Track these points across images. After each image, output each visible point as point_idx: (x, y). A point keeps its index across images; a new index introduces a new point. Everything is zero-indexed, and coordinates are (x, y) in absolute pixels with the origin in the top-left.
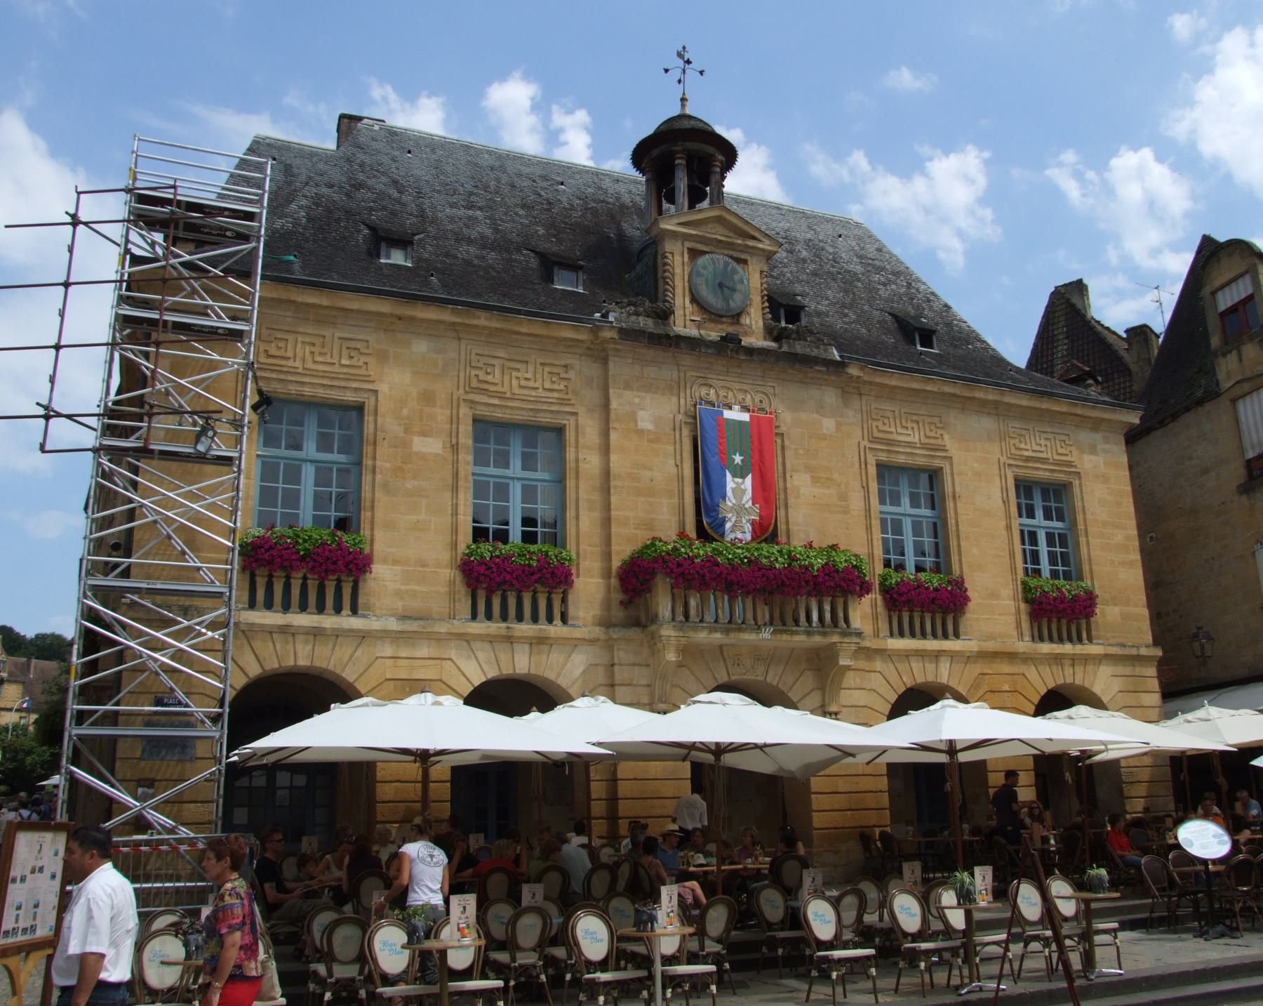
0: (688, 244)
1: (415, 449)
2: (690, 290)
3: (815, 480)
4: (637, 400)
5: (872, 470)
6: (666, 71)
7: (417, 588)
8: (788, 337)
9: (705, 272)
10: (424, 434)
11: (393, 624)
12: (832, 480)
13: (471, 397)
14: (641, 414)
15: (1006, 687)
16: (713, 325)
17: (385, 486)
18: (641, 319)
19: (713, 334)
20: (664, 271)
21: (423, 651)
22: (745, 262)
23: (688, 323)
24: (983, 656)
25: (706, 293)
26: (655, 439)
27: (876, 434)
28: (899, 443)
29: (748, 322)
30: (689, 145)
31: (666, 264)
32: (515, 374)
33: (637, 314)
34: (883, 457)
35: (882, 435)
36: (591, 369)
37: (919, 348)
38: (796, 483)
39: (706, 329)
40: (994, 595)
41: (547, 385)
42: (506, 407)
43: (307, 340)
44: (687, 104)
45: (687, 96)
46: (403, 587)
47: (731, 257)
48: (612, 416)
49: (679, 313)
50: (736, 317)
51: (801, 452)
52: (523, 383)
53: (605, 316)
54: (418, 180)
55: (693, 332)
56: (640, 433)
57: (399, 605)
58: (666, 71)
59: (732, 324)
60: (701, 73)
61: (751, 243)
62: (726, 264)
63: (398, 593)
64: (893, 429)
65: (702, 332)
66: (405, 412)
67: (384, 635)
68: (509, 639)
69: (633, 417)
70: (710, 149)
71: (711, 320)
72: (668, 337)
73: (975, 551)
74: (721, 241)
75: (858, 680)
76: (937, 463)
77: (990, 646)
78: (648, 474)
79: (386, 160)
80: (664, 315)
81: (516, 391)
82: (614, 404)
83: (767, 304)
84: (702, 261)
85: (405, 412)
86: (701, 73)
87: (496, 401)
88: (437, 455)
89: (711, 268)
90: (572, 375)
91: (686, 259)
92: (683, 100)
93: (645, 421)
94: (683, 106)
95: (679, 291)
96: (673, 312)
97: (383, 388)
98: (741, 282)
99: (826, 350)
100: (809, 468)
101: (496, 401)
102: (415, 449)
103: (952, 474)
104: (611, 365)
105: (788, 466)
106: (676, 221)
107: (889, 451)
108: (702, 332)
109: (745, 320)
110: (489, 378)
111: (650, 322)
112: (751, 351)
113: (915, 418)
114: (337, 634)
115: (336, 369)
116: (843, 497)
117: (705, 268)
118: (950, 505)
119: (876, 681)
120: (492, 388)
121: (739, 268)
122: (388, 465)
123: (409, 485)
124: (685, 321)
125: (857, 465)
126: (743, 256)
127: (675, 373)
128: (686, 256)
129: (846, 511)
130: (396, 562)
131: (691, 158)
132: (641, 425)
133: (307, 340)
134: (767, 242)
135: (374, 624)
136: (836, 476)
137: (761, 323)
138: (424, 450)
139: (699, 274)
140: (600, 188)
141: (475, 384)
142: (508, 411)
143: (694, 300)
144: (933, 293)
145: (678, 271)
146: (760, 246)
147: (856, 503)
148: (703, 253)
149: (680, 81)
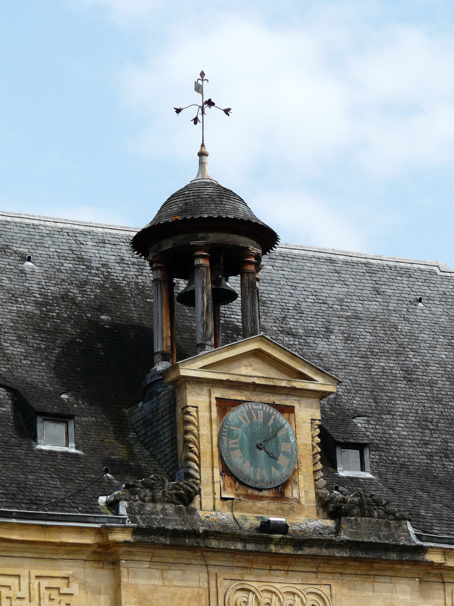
0: (218, 393)
2: (221, 457)
6: (178, 111)
8: (347, 514)
9: (239, 431)
16: (250, 503)
18: (159, 507)
19: (249, 517)
20: (187, 432)
22: (290, 410)
23: (218, 502)
25: (240, 461)
29: (295, 495)
30: (213, 238)
31: (188, 422)
33: (154, 500)
36: (100, 577)
44: (207, 160)
45: (207, 149)
47: (273, 405)
49: (206, 489)
50: (280, 492)
53: (113, 506)
55: (224, 515)
58: (178, 111)
59: (274, 499)
60: (227, 111)
61: (299, 384)
62: (267, 417)
65: (237, 514)
70: (243, 241)
72: (194, 534)
74: (259, 385)
80: (186, 497)
83: (320, 466)
84: (235, 415)
86: (227, 111)
89: (245, 424)
90: (74, 588)
91: (215, 414)
92: (202, 154)
94: (202, 164)
95: (206, 460)
96: (199, 492)
98: (287, 440)
104: (124, 572)
106: (201, 363)
108: (237, 514)
109: (292, 492)
111: (170, 508)
112: (301, 541)
117: (239, 425)
121: (282, 419)
126: (288, 403)
127: (205, 576)
128: (214, 409)
134: (319, 379)
137: (312, 495)
139: (231, 435)
140: (80, 259)
143: (226, 471)
145: (204, 431)
146: (311, 386)
148: (237, 403)
149: (196, 120)
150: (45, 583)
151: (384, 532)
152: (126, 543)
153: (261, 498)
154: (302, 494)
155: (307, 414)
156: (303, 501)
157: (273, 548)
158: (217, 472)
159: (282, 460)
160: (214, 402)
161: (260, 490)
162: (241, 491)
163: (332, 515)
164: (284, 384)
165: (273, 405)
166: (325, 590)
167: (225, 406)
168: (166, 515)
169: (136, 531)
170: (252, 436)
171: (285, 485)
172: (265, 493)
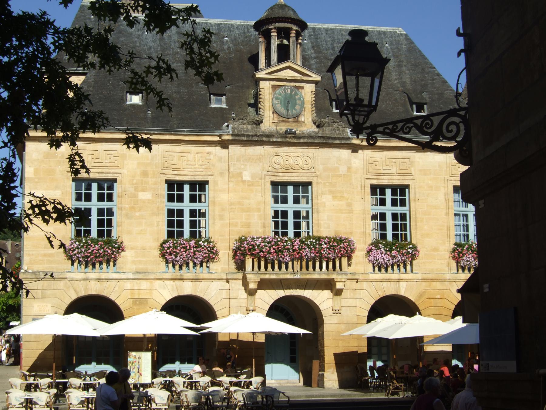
1: (140, 198)
3: (334, 198)
4: (243, 167)
5: (369, 190)
7: (142, 259)
8: (323, 126)
10: (143, 190)
11: (131, 276)
12: (343, 197)
13: (164, 171)
14: (245, 173)
15: (439, 296)
17: (127, 215)
18: (245, 126)
19: (283, 128)
21: (145, 285)
23: (271, 124)
24: (424, 280)
26: (251, 184)
27: (371, 171)
28: (384, 175)
29: (303, 120)
32: (185, 159)
34: (375, 182)
35: (374, 171)
37: (415, 113)
38: (324, 200)
39: (280, 126)
40: (436, 249)
41: (201, 163)
42: (180, 175)
43: (90, 152)
46: (136, 259)
48: (230, 175)
50: (296, 118)
51: (327, 184)
52: (189, 163)
54: (150, 48)
55: (273, 128)
56: (244, 182)
57: (134, 267)
59: (294, 122)
63: (134, 262)
64: (381, 168)
66: (135, 181)
67: (128, 279)
68: (182, 280)
69: (240, 175)
71: (283, 121)
73: (426, 227)
75: (352, 295)
76: (406, 183)
77: (429, 276)
78: (247, 201)
79: (135, 38)
80: (259, 123)
81: (186, 167)
82: (231, 170)
83: (314, 109)
85: (135, 181)
87: (176, 173)
88: (149, 200)
93: (247, 176)
97: (125, 171)
99: (343, 131)
100: (331, 192)
101: (176, 173)
102: (140, 198)
103: (415, 188)
105: (320, 192)
107: (378, 179)
109: (302, 119)
110: (172, 162)
111: (249, 127)
113: (393, 160)
114: (107, 280)
115: (104, 164)
116: (349, 205)
118: (412, 204)
119: (363, 294)
120: (173, 167)
122: (127, 206)
123: (137, 214)
124: (269, 122)
125: (359, 188)
128: (271, 89)
129: (351, 212)
130: (132, 249)
131: (279, 31)
132: (245, 178)
133: (90, 152)
135: (123, 276)
136: (345, 195)
137: (310, 120)
138: (143, 198)
141: (166, 165)
142: (181, 177)
143: (275, 112)
144: (438, 74)
146: (310, 79)
147: (358, 207)
150: (200, 155)
151: (337, 132)
152: (229, 140)
153: (288, 122)
154: (306, 120)
155: (310, 88)
156: (306, 122)
157: (288, 140)
158: (271, 112)
159: (297, 107)
160: (271, 86)
161: (289, 118)
162: (281, 119)
163: (318, 126)
164: (299, 78)
165: (295, 87)
166: (310, 155)
167: (274, 87)
168: (249, 128)
169: (232, 135)
170: (285, 99)
171: (298, 116)
172: (290, 120)
